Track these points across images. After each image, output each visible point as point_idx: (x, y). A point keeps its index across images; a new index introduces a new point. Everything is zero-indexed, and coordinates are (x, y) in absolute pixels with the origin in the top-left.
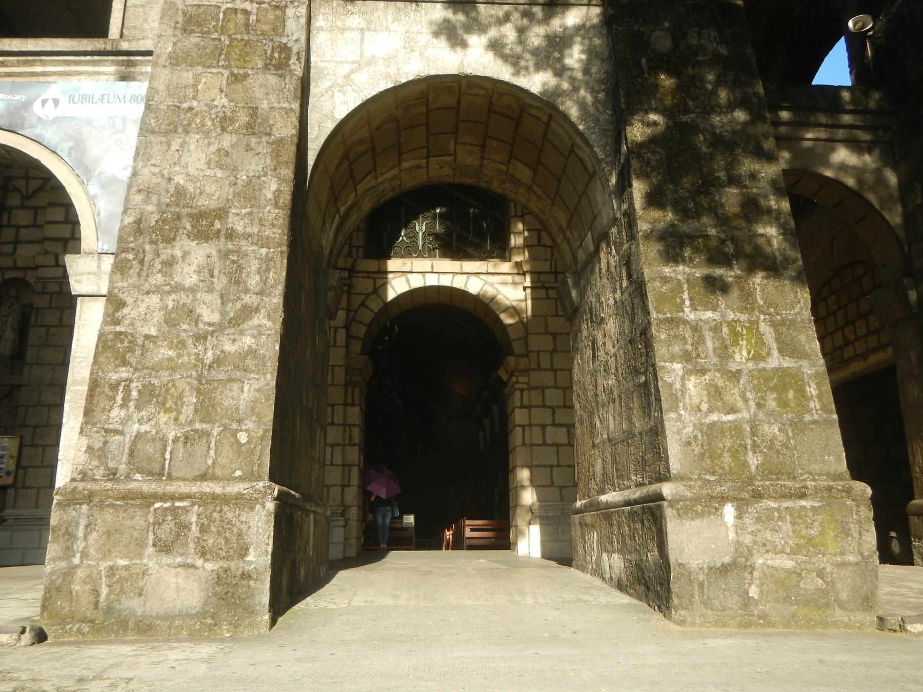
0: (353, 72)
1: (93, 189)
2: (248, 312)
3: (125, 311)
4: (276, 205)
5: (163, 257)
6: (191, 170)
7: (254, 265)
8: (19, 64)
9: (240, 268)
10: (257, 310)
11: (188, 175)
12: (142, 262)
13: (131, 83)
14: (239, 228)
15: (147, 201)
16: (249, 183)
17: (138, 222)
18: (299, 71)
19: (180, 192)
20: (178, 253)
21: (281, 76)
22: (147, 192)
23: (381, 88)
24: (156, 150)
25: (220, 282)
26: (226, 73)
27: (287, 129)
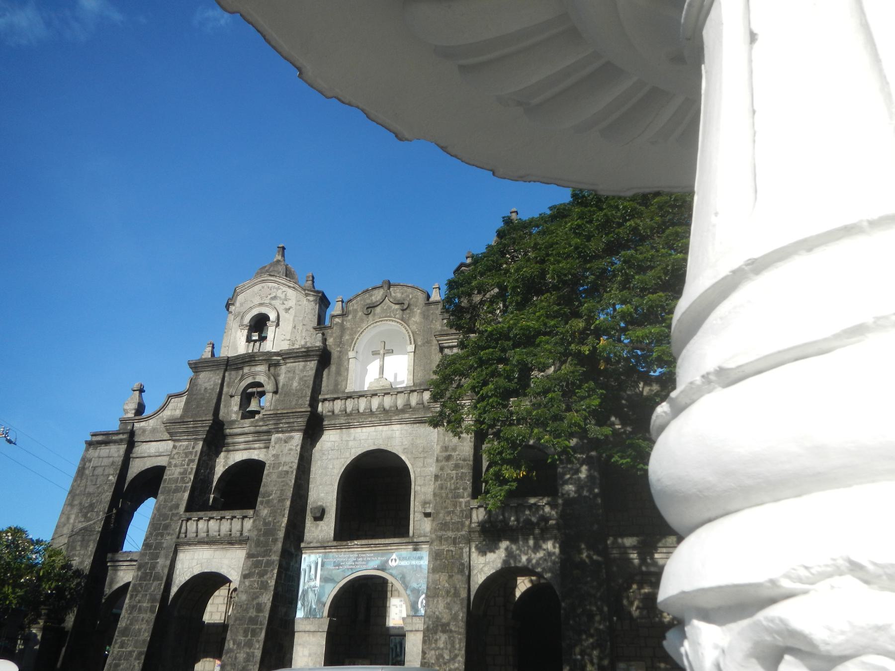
0: (483, 567)
1: (409, 592)
2: (456, 656)
3: (426, 655)
4: (462, 621)
5: (435, 638)
6: (440, 610)
7: (457, 641)
8: (383, 547)
9: (454, 642)
10: (458, 655)
11: (439, 611)
12: (429, 640)
13: (418, 552)
14: (453, 629)
15: (429, 620)
16: (455, 614)
17: (428, 627)
18: (467, 573)
19: (438, 617)
20: (438, 637)
21: (463, 575)
22: (429, 617)
23: (491, 572)
24: (431, 603)
25: (449, 647)
26: (447, 575)
27: (464, 594)
